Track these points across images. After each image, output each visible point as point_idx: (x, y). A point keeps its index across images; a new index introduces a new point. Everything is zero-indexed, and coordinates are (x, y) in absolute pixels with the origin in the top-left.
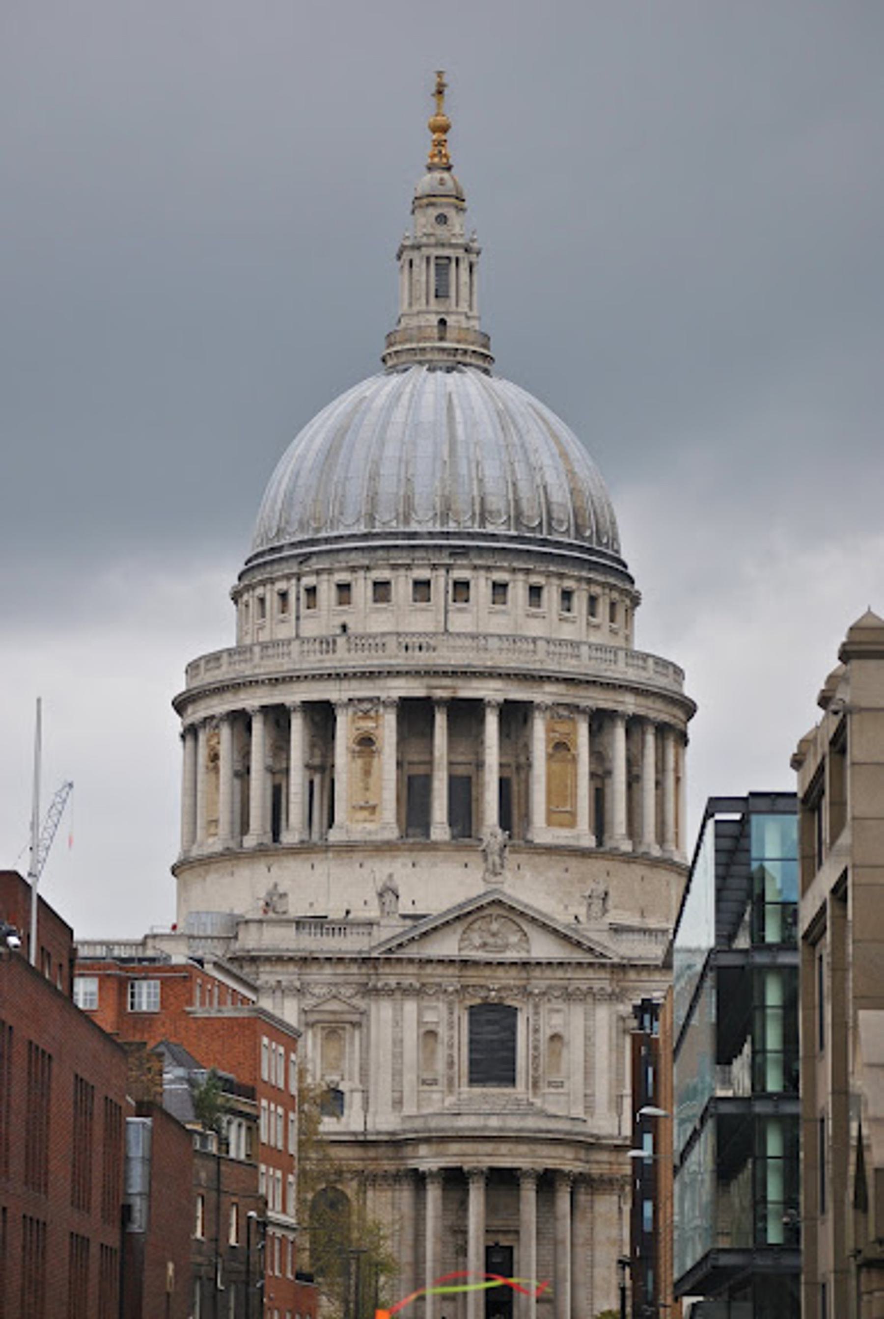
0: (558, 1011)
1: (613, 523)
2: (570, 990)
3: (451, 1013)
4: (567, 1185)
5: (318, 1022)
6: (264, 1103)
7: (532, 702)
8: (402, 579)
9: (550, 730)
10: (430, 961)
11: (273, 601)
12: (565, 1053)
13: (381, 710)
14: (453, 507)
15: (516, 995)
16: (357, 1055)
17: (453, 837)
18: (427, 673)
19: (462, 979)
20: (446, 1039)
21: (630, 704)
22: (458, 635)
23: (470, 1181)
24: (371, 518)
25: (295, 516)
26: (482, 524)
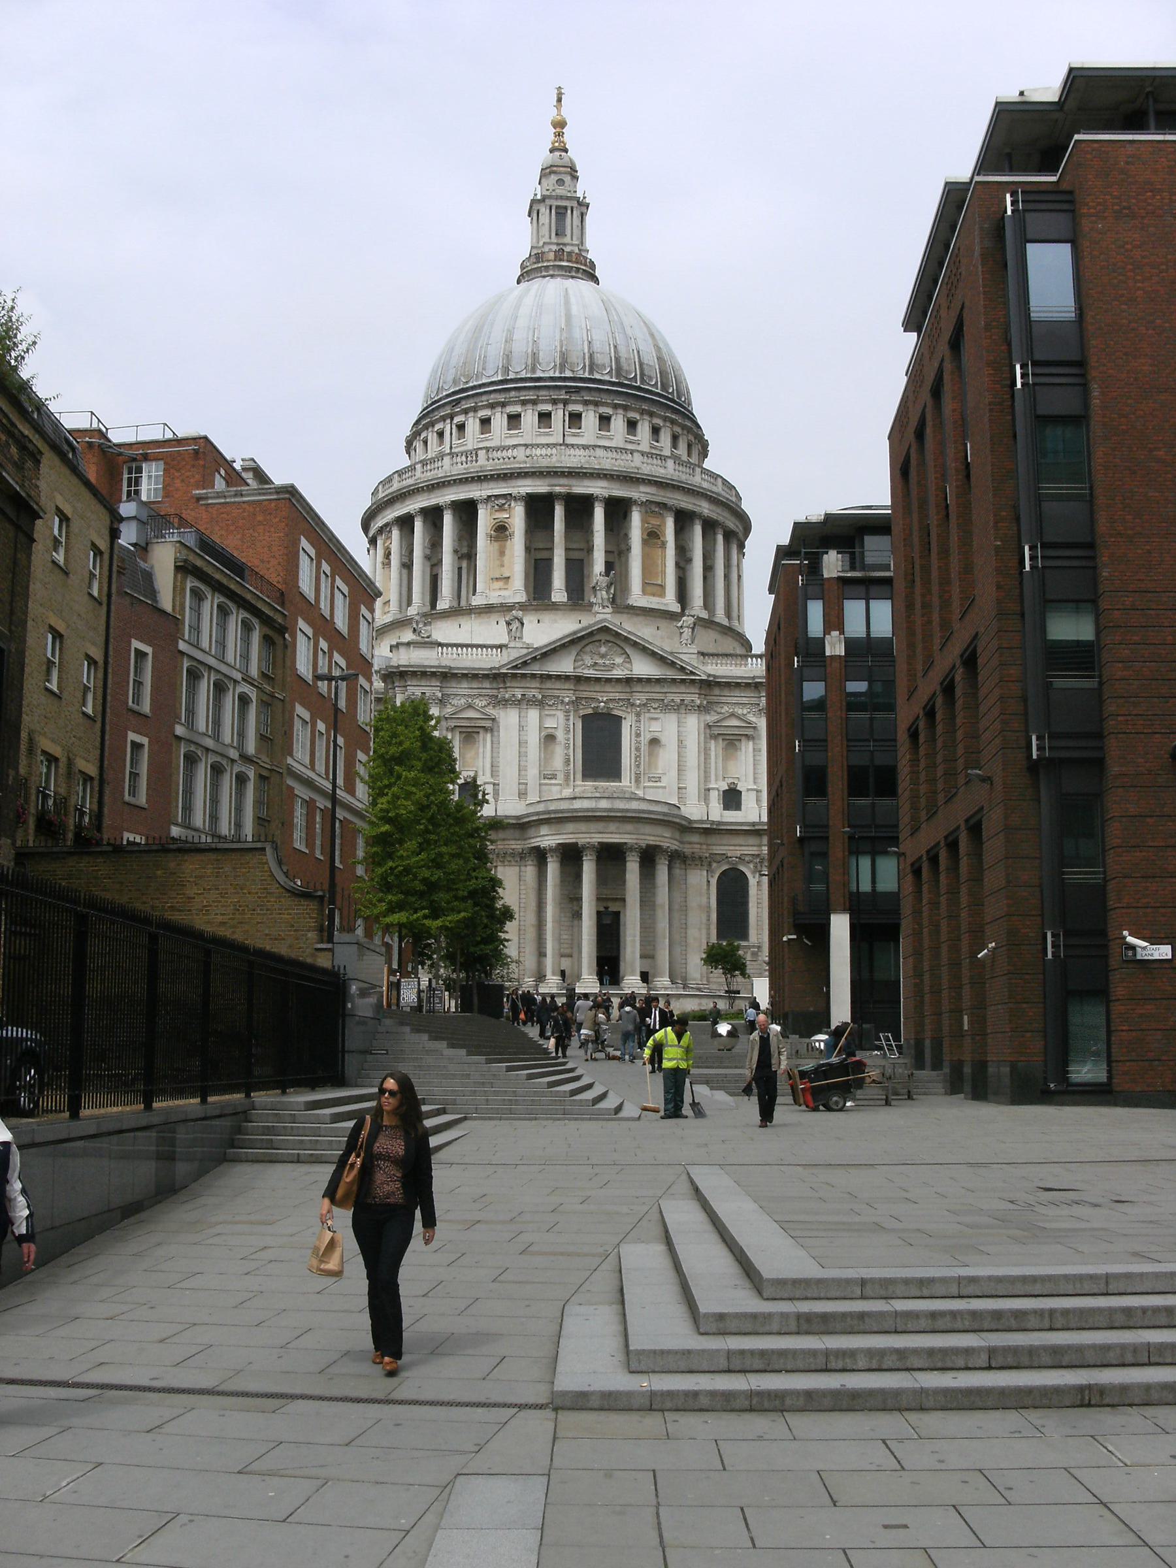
0: (656, 719)
1: (688, 392)
3: (568, 720)
6: (301, 624)
10: (549, 677)
11: (432, 438)
14: (569, 361)
16: (488, 754)
17: (569, 598)
18: (549, 473)
20: (564, 742)
21: (705, 508)
22: (573, 446)
24: (506, 370)
25: (450, 378)
26: (591, 372)
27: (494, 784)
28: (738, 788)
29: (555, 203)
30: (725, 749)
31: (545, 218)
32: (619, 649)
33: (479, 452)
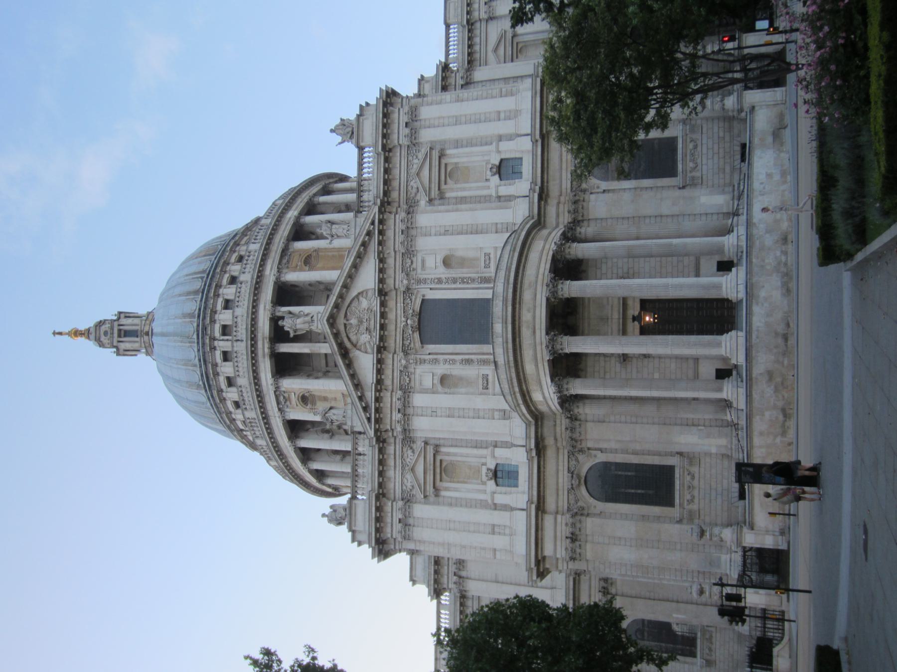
0: (423, 261)
2: (404, 251)
3: (425, 361)
4: (569, 247)
5: (434, 487)
7: (275, 283)
8: (223, 369)
9: (295, 269)
10: (379, 382)
12: (460, 253)
13: (283, 389)
15: (411, 300)
18: (253, 358)
19: (397, 350)
20: (447, 366)
21: (292, 214)
23: (561, 352)
27: (496, 446)
28: (497, 163)
29: (116, 339)
30: (456, 182)
31: (128, 346)
32: (353, 305)
33: (247, 417)
